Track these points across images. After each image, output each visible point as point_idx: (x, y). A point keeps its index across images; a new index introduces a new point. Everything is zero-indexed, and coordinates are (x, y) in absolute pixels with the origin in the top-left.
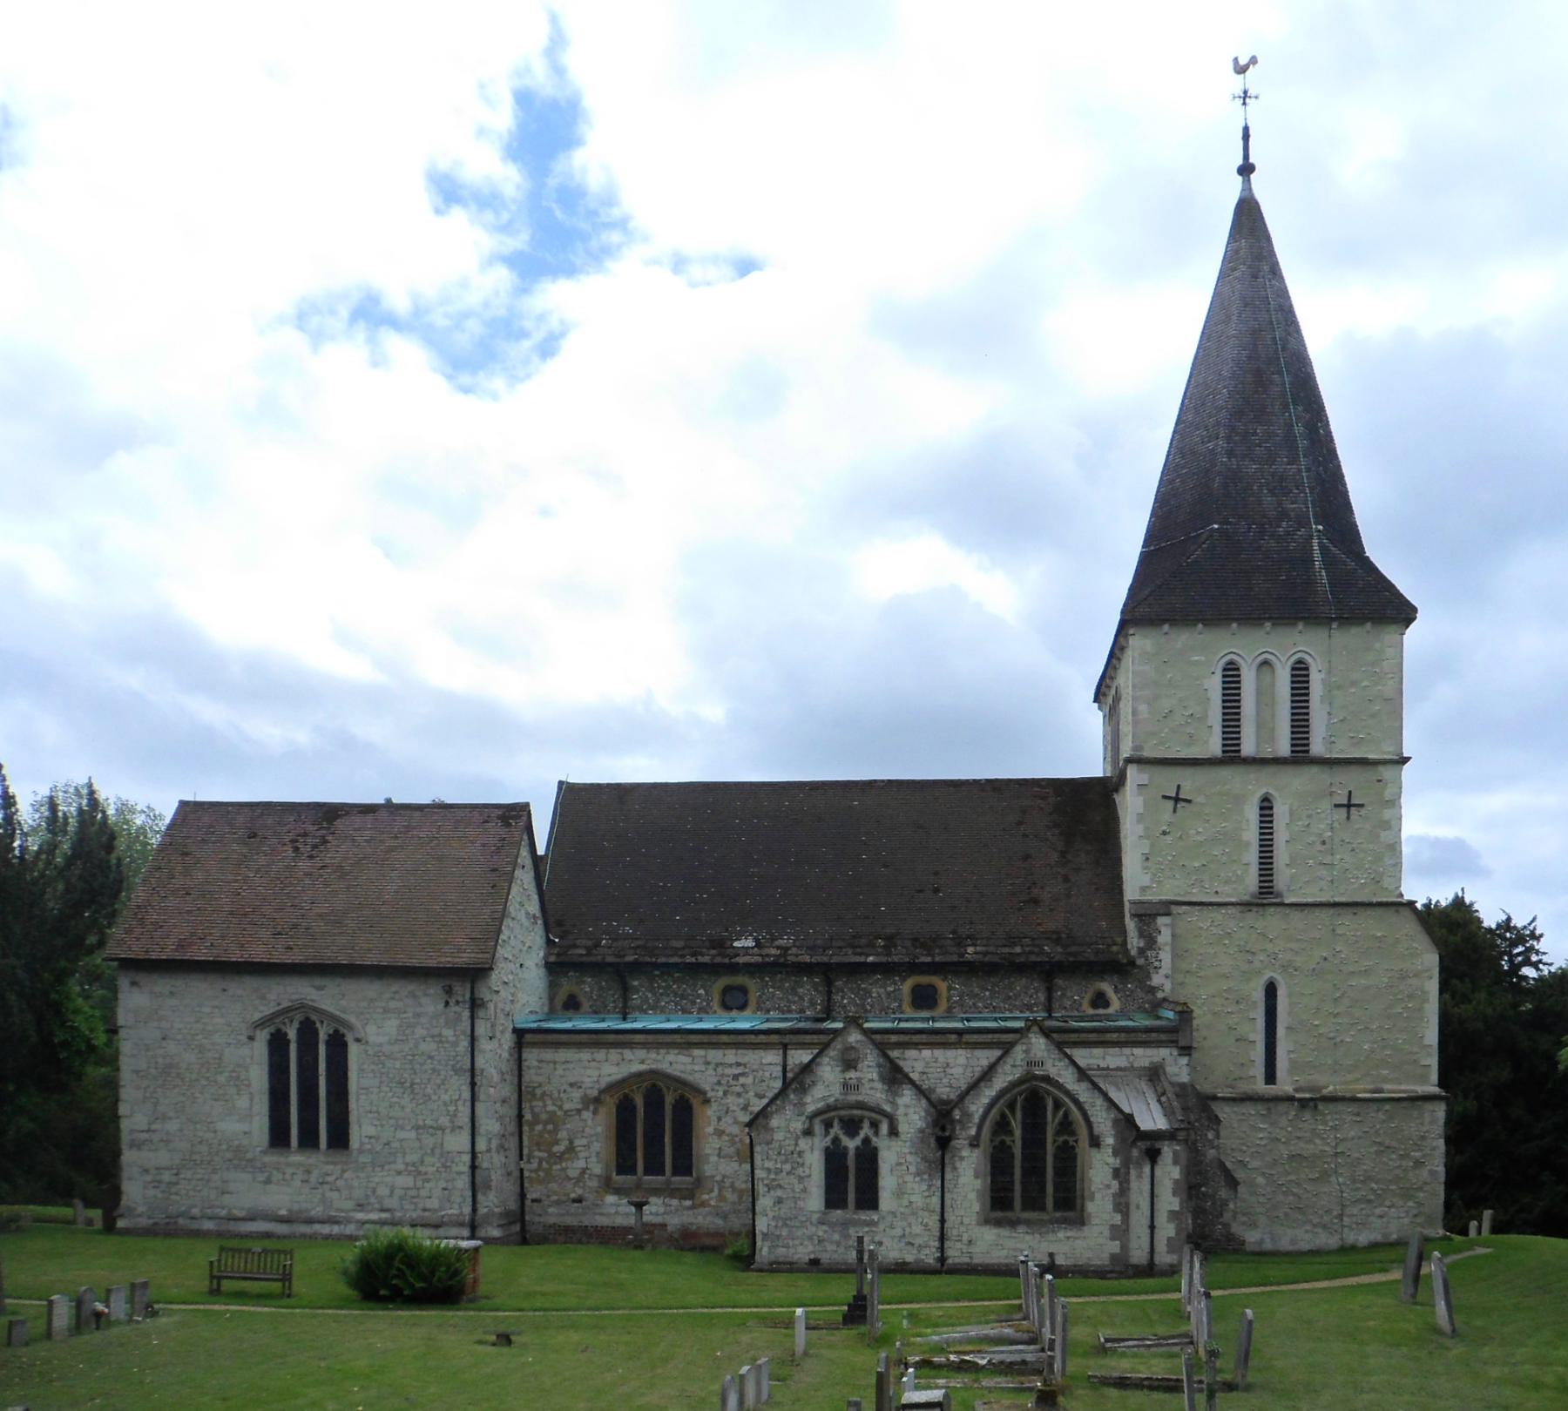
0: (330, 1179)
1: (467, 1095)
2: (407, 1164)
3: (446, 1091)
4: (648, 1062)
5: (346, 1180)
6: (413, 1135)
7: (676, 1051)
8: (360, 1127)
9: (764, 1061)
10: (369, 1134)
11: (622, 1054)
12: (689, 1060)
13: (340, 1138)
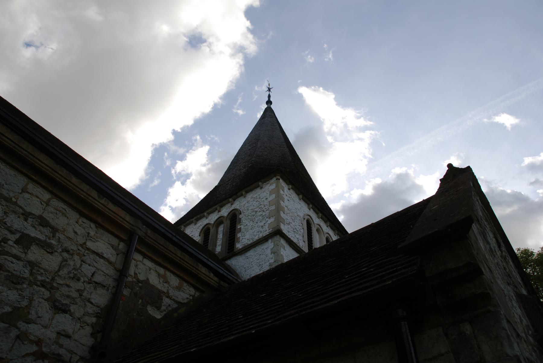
9: (89, 244)
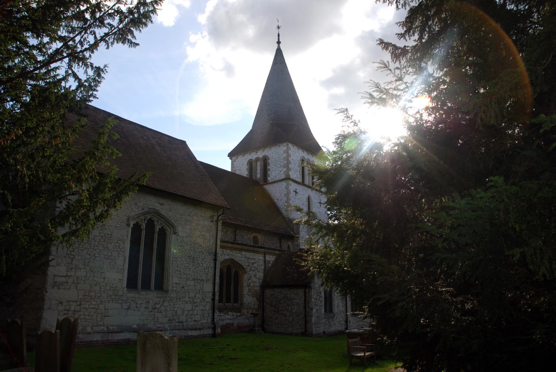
0: (157, 306)
1: (212, 265)
2: (190, 298)
3: (205, 262)
4: (230, 255)
5: (165, 306)
6: (192, 283)
7: (238, 252)
8: (173, 278)
9: (259, 258)
10: (176, 282)
11: (223, 251)
12: (241, 256)
13: (160, 286)
